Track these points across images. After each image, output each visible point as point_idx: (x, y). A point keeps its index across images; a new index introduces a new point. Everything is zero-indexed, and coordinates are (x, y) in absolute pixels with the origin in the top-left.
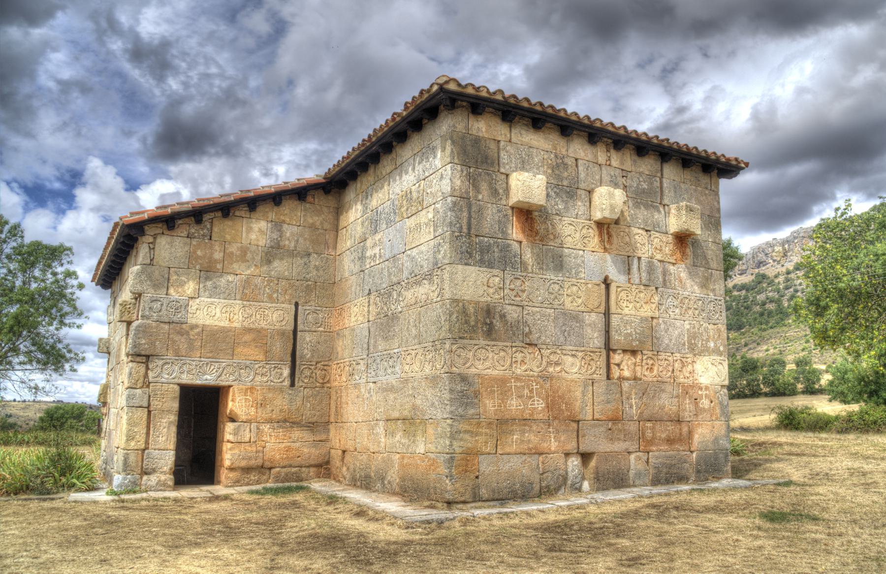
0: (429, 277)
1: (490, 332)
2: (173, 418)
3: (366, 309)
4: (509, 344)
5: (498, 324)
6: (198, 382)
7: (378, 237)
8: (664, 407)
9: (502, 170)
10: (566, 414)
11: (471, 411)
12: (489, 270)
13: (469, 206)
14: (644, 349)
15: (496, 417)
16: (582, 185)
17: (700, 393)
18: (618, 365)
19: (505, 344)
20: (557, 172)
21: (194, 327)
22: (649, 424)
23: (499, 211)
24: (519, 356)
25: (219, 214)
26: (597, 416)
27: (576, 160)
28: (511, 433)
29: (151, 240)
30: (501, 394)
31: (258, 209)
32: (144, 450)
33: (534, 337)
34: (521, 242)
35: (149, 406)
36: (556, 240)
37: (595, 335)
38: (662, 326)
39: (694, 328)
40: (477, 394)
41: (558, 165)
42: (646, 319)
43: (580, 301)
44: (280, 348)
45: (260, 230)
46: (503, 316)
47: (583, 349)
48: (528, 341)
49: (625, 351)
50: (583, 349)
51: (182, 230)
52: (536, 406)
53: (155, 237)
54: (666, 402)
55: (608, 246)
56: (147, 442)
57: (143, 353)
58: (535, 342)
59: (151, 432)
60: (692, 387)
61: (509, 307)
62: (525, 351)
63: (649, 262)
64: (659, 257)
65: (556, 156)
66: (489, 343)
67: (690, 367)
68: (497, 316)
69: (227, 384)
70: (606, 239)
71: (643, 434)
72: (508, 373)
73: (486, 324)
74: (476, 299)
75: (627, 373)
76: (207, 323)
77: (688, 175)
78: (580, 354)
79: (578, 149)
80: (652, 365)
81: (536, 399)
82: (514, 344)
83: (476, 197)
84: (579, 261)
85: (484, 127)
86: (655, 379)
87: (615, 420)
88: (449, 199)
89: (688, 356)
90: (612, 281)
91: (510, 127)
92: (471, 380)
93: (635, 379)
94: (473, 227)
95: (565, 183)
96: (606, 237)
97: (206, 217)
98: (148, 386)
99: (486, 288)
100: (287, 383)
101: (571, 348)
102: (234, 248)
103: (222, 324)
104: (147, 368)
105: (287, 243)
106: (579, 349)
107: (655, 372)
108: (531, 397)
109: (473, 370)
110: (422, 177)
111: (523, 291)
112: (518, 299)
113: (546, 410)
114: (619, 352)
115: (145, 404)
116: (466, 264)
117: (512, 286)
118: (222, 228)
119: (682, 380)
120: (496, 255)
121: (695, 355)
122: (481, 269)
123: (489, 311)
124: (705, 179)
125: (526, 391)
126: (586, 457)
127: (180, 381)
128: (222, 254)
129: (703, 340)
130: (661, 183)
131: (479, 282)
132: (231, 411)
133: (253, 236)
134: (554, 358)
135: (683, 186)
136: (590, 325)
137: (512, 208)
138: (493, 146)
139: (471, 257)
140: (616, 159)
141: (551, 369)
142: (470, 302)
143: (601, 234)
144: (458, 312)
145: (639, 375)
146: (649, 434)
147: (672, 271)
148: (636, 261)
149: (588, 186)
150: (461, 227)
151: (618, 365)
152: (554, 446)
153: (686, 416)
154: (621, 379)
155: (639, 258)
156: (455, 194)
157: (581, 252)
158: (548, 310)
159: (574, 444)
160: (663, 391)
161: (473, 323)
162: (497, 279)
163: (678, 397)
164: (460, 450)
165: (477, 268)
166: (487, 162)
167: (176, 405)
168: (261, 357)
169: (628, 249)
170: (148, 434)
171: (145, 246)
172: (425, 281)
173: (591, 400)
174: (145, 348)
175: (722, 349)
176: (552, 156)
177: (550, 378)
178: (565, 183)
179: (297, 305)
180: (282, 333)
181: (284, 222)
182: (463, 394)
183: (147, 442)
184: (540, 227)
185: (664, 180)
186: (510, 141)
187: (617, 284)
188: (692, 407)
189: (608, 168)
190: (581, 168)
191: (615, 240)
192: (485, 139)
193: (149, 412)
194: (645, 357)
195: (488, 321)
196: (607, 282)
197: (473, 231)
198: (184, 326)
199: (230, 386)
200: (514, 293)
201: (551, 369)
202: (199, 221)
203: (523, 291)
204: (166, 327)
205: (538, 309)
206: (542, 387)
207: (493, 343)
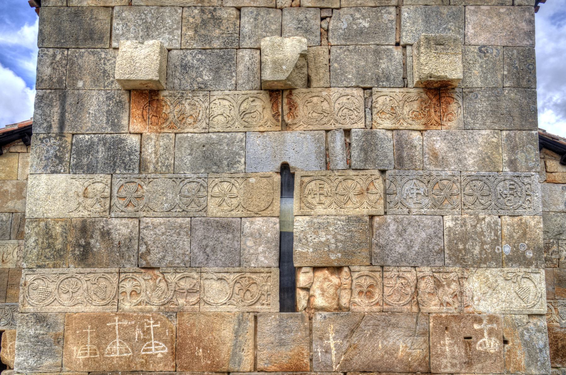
1: (85, 256)
4: (115, 270)
5: (97, 243)
12: (89, 176)
14: (353, 264)
17: (476, 326)
18: (307, 289)
19: (109, 270)
20: (202, 32)
23: (109, 98)
24: (128, 286)
26: (261, 365)
27: (239, 9)
30: (98, 336)
33: (153, 259)
34: (141, 134)
36: (198, 124)
37: (261, 249)
38: (392, 227)
39: (464, 224)
40: (60, 340)
41: (204, 23)
42: (359, 219)
43: (235, 202)
46: (106, 234)
47: (238, 269)
48: (144, 263)
50: (238, 269)
52: (153, 352)
54: (401, 346)
55: (289, 121)
58: (157, 265)
60: (458, 318)
61: (115, 221)
62: (139, 277)
63: (366, 134)
65: (202, 11)
66: (82, 270)
67: (454, 286)
68: (97, 235)
72: (111, 309)
73: (80, 246)
74: (65, 214)
75: (319, 301)
78: (232, 277)
80: (371, 286)
82: (122, 270)
84: (235, 148)
86: (376, 308)
89: (451, 269)
90: (294, 169)
92: (51, 320)
93: (340, 308)
94: (67, 124)
95: (216, 44)
96: (286, 107)
99: (81, 199)
101: (216, 269)
106: (231, 269)
107: (377, 297)
108: (145, 341)
109: (56, 308)
111: (140, 198)
112: (130, 208)
113: (170, 358)
114: (304, 270)
116: (53, 172)
117: (124, 194)
120: (100, 155)
121: (465, 267)
122: (76, 176)
123: (85, 228)
125: (138, 332)
129: (483, 243)
130: (399, 15)
131: (71, 194)
134: (185, 285)
135: (445, 10)
136: (252, 235)
139: (61, 162)
141: (181, 301)
142: (56, 220)
144: (37, 234)
145: (344, 301)
147: (416, 143)
149: (256, 42)
150: (50, 127)
151: (307, 289)
155: (347, 132)
156: (43, 86)
157: (240, 136)
158: (179, 220)
161: (59, 246)
162: (99, 186)
165: (71, 175)
166: (92, 38)
169: (325, 120)
173: (251, 343)
175: (529, 254)
176: (196, 11)
177: (179, 313)
178: (216, 44)
182: (38, 340)
184: (170, 110)
185: (404, 9)
187: (304, 173)
188: (460, 351)
189: (294, 11)
191: (302, 111)
192: (91, 9)
194: (355, 275)
195: (82, 242)
197: (68, 130)
200: (126, 201)
201: (181, 301)
203: (140, 198)
205: (162, 220)
206: (164, 325)
207: (88, 270)
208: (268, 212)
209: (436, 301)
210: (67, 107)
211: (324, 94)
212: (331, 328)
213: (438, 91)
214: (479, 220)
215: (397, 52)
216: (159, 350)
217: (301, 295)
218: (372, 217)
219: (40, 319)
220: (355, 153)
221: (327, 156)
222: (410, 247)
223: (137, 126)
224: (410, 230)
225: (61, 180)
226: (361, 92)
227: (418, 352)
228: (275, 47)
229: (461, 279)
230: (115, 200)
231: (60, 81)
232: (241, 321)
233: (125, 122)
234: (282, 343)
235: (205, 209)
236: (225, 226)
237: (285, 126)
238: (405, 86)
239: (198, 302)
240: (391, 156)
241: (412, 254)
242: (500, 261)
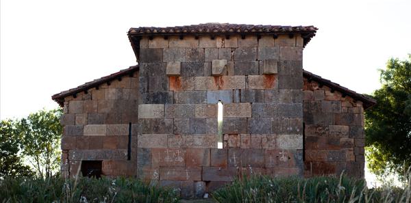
1: (157, 130)
5: (160, 126)
11: (147, 163)
16: (206, 60)
18: (226, 141)
21: (86, 137)
24: (171, 140)
28: (166, 172)
42: (243, 119)
44: (124, 143)
45: (113, 93)
46: (164, 123)
51: (80, 96)
53: (68, 101)
60: (275, 150)
72: (166, 147)
77: (277, 41)
83: (152, 75)
84: (204, 96)
87: (223, 166)
100: (127, 158)
103: (97, 135)
107: (249, 144)
119: (267, 147)
121: (277, 134)
123: (156, 121)
125: (174, 154)
126: (207, 183)
130: (257, 49)
133: (110, 96)
134: (188, 140)
138: (160, 51)
140: (227, 43)
143: (216, 81)
145: (238, 145)
148: (237, 92)
152: (188, 177)
153: (270, 165)
155: (240, 90)
159: (200, 176)
175: (298, 130)
177: (185, 149)
179: (130, 124)
180: (124, 136)
181: (123, 88)
188: (275, 161)
190: (206, 52)
192: (156, 49)
197: (150, 91)
202: (86, 93)
209: (267, 145)
211: (232, 77)
212: (234, 153)
213: (270, 76)
214: (282, 119)
215: (256, 63)
216: (181, 160)
218: (247, 118)
219: (144, 149)
220: (242, 97)
222: (260, 128)
223: (172, 88)
224: (260, 122)
225: (149, 105)
227: (262, 161)
228: (216, 63)
229: (275, 138)
230: (166, 113)
231: (147, 74)
232: (206, 151)
234: (219, 158)
235: (194, 116)
236: (201, 121)
237: (220, 88)
240: (254, 98)
241: (260, 130)
242: (290, 133)
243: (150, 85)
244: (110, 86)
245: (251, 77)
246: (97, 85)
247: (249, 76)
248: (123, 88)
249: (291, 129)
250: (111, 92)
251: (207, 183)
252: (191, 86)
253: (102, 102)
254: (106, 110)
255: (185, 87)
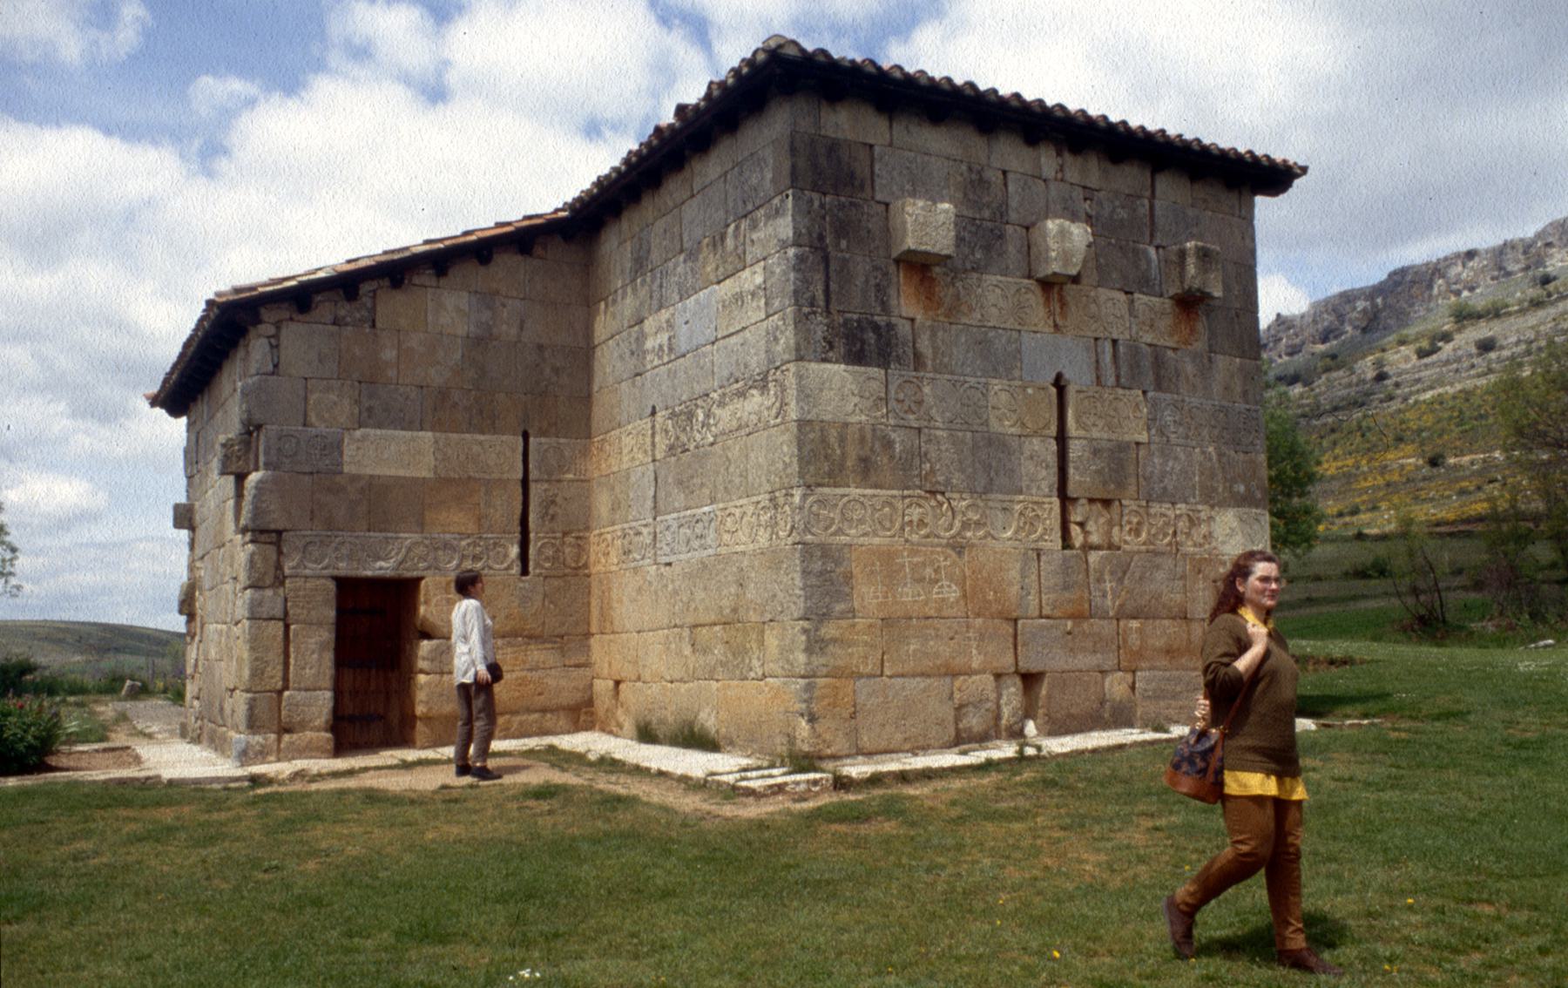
0: (762, 384)
1: (866, 470)
2: (326, 635)
3: (648, 440)
6: (369, 573)
7: (665, 315)
8: (1160, 596)
9: (879, 197)
10: (995, 608)
11: (839, 607)
13: (826, 260)
15: (881, 615)
16: (1013, 216)
19: (895, 492)
21: (355, 478)
22: (1135, 624)
24: (915, 513)
25: (386, 282)
27: (1005, 173)
29: (271, 330)
31: (451, 272)
32: (280, 693)
35: (286, 613)
49: (1091, 501)
51: (325, 308)
53: (278, 325)
55: (1060, 322)
56: (286, 679)
57: (273, 526)
59: (292, 661)
64: (1148, 338)
65: (970, 169)
69: (415, 574)
70: (1058, 310)
71: (1125, 641)
75: (1095, 539)
76: (377, 472)
77: (1201, 191)
79: (1008, 154)
80: (1139, 523)
81: (946, 583)
85: (844, 123)
88: (791, 252)
91: (891, 120)
93: (1111, 546)
94: (834, 297)
97: (365, 288)
98: (282, 583)
100: (516, 570)
101: (1000, 497)
102: (414, 341)
103: (401, 473)
104: (280, 553)
105: (504, 327)
108: (937, 581)
110: (741, 212)
113: (962, 603)
115: (278, 612)
116: (824, 360)
117: (901, 396)
118: (392, 305)
121: (1212, 507)
124: (1229, 199)
125: (929, 571)
126: (1030, 680)
127: (336, 573)
128: (395, 353)
132: (425, 619)
133: (445, 319)
137: (897, 261)
143: (1048, 300)
145: (1116, 539)
146: (1134, 641)
148: (1108, 347)
154: (1088, 547)
155: (1115, 342)
160: (1158, 567)
163: (1183, 577)
164: (825, 671)
167: (331, 614)
168: (472, 527)
170: (286, 664)
171: (264, 341)
172: (754, 392)
174: (277, 520)
179: (526, 436)
183: (286, 679)
184: (945, 294)
185: (1157, 203)
186: (891, 145)
190: (1011, 188)
193: (287, 627)
196: (1060, 384)
197: (834, 307)
198: (338, 478)
199: (420, 579)
204: (307, 478)
208: (1047, 432)
210: (832, 274)
217: (1075, 530)
218: (1138, 444)
220: (1124, 370)
221: (1097, 368)
226: (1122, 297)
227: (1178, 597)
233: (894, 302)
234: (1066, 587)
235: (986, 423)
238: (1161, 296)
239: (985, 537)
243: (833, 286)
244: (443, 281)
245: (1141, 299)
246: (396, 272)
247: (1136, 295)
248: (497, 292)
249: (1242, 488)
250: (450, 309)
251: (1030, 680)
252: (971, 309)
253: (414, 341)
254: (437, 376)
255: (953, 311)
